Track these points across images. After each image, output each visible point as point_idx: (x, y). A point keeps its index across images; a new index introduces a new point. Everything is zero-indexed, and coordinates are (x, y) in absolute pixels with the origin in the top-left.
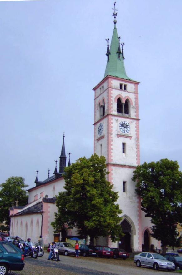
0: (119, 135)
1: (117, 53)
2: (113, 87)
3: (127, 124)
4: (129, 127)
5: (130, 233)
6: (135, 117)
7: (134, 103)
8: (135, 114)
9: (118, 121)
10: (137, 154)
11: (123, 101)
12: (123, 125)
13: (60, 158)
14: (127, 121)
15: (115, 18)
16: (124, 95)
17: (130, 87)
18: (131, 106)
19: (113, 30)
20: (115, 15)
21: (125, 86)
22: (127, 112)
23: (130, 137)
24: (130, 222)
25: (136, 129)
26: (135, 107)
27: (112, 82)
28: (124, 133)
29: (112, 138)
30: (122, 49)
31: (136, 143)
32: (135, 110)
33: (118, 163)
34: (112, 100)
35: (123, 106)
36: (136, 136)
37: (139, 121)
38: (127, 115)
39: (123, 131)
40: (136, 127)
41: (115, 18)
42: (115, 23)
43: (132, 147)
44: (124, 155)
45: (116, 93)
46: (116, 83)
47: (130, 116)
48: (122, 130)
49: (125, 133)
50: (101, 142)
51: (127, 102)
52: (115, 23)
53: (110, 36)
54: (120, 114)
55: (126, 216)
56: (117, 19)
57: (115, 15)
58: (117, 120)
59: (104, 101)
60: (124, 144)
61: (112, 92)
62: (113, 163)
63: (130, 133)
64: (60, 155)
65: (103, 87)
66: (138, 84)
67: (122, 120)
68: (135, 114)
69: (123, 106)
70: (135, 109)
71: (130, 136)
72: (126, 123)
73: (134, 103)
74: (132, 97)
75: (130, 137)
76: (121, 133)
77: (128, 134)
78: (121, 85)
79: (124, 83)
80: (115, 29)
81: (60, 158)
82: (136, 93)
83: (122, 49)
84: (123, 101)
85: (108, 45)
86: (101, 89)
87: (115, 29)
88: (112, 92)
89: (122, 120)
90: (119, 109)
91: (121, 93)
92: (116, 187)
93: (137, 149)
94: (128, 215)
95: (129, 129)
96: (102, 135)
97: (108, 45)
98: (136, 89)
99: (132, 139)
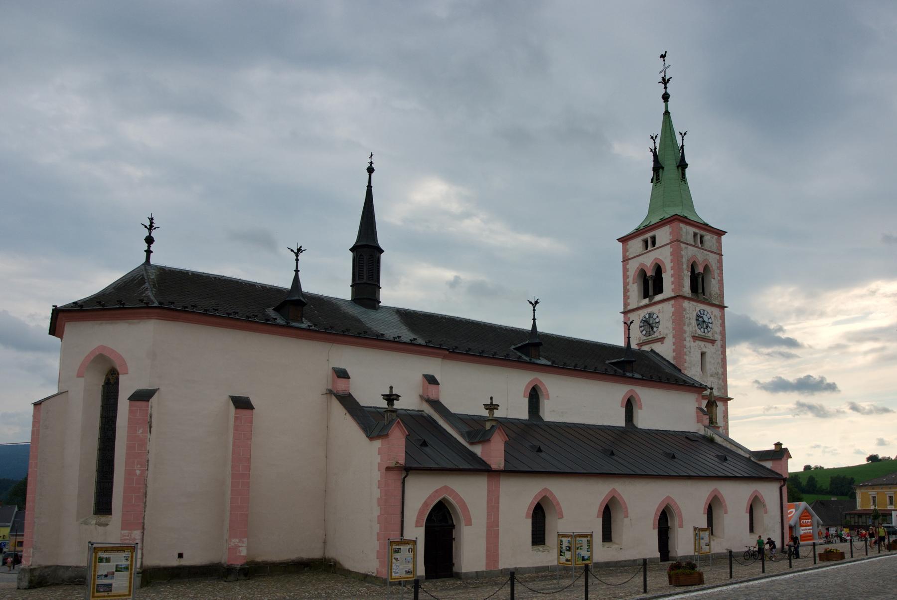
11: (700, 269)
15: (666, 88)
16: (701, 256)
19: (661, 117)
20: (665, 82)
21: (702, 237)
41: (666, 88)
42: (666, 97)
51: (706, 268)
52: (666, 97)
53: (658, 130)
56: (668, 91)
57: (665, 82)
59: (659, 270)
65: (654, 239)
77: (710, 335)
78: (695, 235)
80: (667, 113)
86: (646, 242)
87: (667, 113)
96: (656, 335)
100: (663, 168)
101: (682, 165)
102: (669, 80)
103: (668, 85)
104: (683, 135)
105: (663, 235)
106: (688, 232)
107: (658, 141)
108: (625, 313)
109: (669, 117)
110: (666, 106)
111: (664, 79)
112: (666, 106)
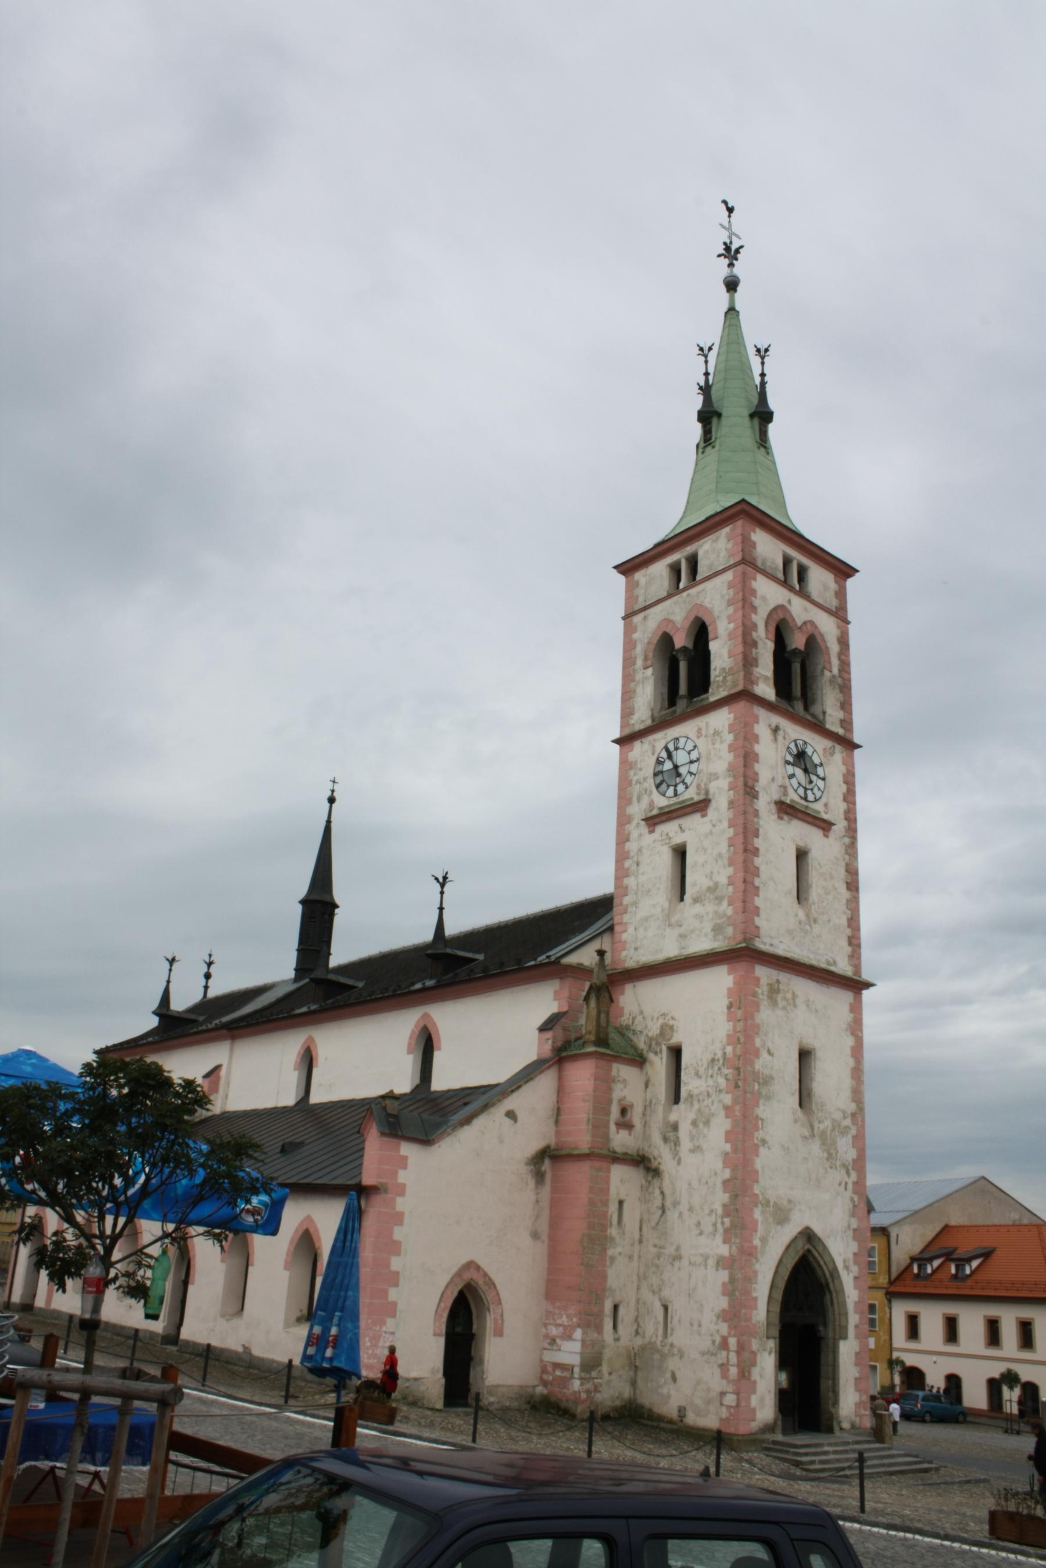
1: (752, 416)
2: (759, 564)
3: (816, 760)
5: (821, 1328)
9: (781, 733)
11: (797, 642)
13: (303, 902)
18: (827, 673)
20: (731, 253)
26: (840, 680)
28: (803, 802)
29: (756, 813)
34: (755, 626)
37: (857, 752)
41: (731, 265)
50: (691, 831)
54: (784, 704)
64: (302, 889)
66: (849, 576)
67: (794, 736)
71: (825, 817)
77: (818, 807)
80: (732, 311)
81: (303, 902)
82: (840, 614)
87: (732, 311)
92: (772, 1078)
95: (821, 783)
98: (841, 594)
100: (719, 415)
101: (762, 416)
102: (737, 251)
104: (762, 353)
105: (716, 550)
106: (768, 548)
107: (712, 356)
108: (627, 617)
109: (738, 326)
110: (732, 300)
111: (728, 248)
112: (732, 300)
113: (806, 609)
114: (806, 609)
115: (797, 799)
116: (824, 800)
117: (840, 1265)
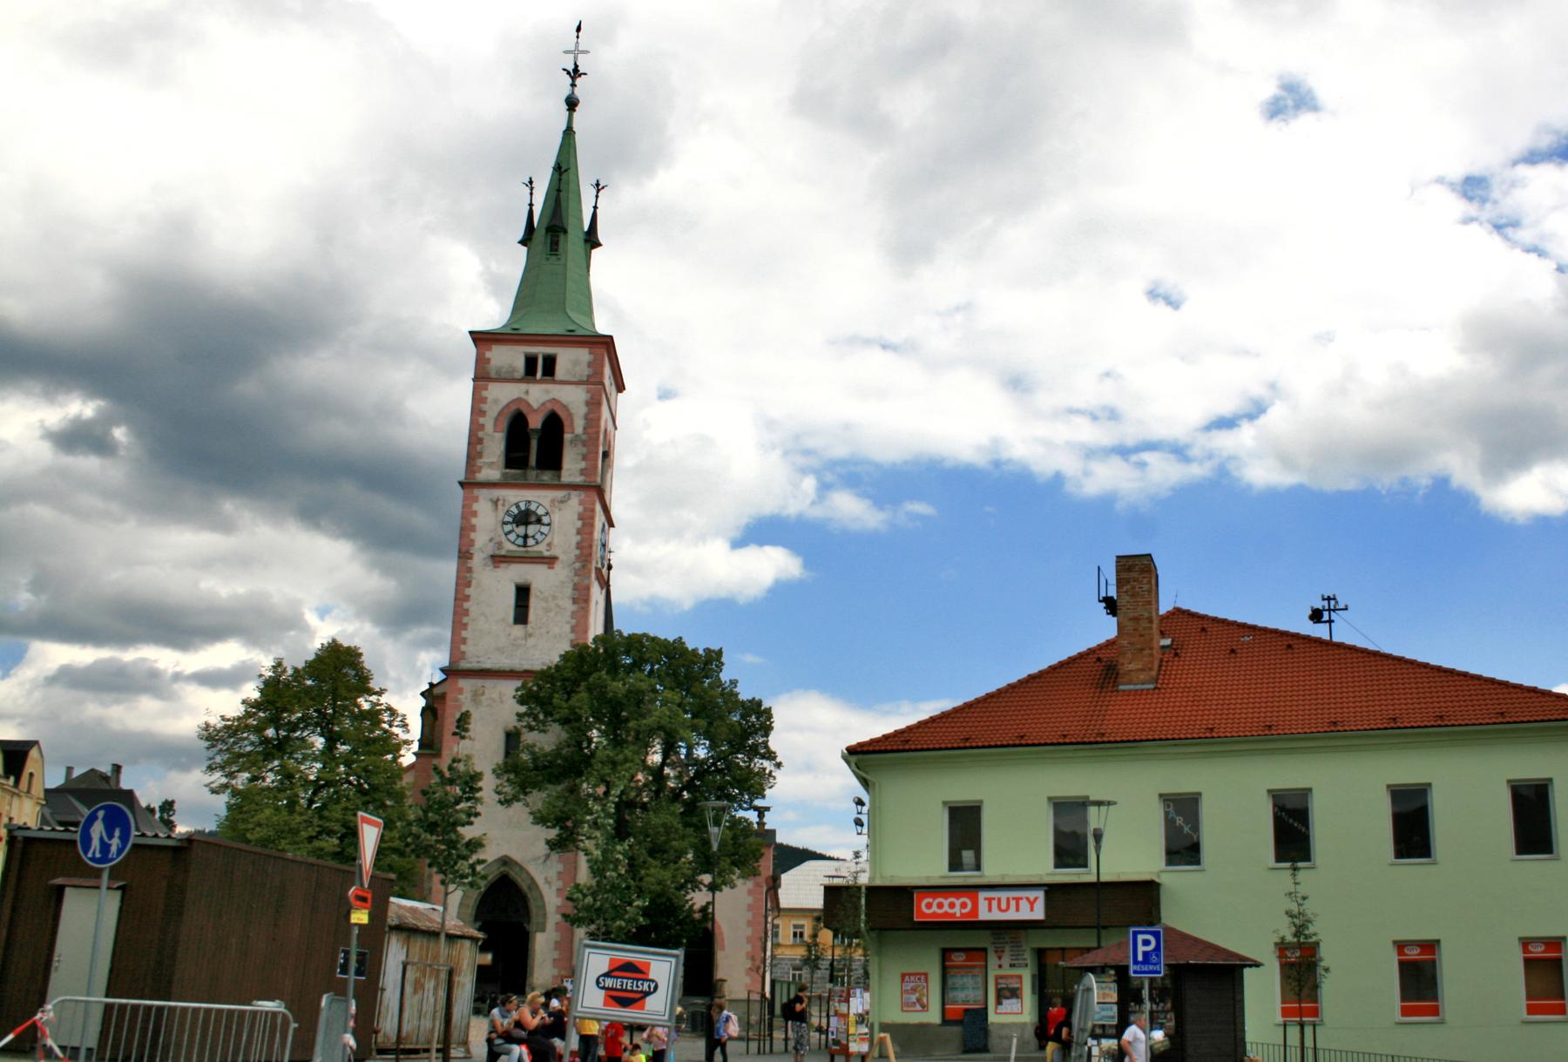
0: (498, 560)
2: (493, 375)
3: (541, 511)
4: (545, 520)
6: (579, 479)
7: (579, 425)
8: (583, 465)
10: (574, 622)
11: (535, 422)
12: (525, 518)
14: (539, 499)
15: (573, 85)
16: (537, 395)
17: (570, 360)
18: (567, 437)
22: (551, 459)
23: (550, 561)
24: (524, 886)
25: (579, 524)
27: (488, 355)
30: (595, 207)
31: (576, 579)
32: (584, 450)
33: (487, 665)
34: (482, 427)
35: (534, 444)
36: (578, 552)
38: (547, 477)
39: (520, 541)
40: (581, 517)
41: (573, 85)
42: (572, 104)
43: (555, 598)
44: (518, 630)
45: (502, 395)
46: (511, 357)
47: (559, 477)
48: (512, 537)
49: (525, 545)
51: (554, 424)
52: (572, 104)
55: (505, 861)
57: (575, 73)
58: (495, 503)
60: (523, 592)
61: (485, 393)
62: (464, 665)
63: (549, 545)
67: (514, 500)
68: (583, 465)
69: (534, 444)
70: (584, 444)
71: (547, 554)
72: (533, 507)
73: (579, 425)
74: (572, 398)
75: (550, 561)
76: (509, 547)
77: (542, 548)
79: (540, 350)
80: (569, 132)
83: (595, 207)
84: (535, 422)
85: (531, 205)
87: (569, 132)
88: (485, 393)
89: (516, 498)
90: (515, 456)
91: (527, 392)
93: (575, 601)
94: (516, 856)
95: (545, 529)
97: (531, 205)
99: (558, 566)
103: (578, 81)
113: (547, 392)
114: (547, 392)
115: (513, 547)
116: (548, 540)
117: (540, 881)
